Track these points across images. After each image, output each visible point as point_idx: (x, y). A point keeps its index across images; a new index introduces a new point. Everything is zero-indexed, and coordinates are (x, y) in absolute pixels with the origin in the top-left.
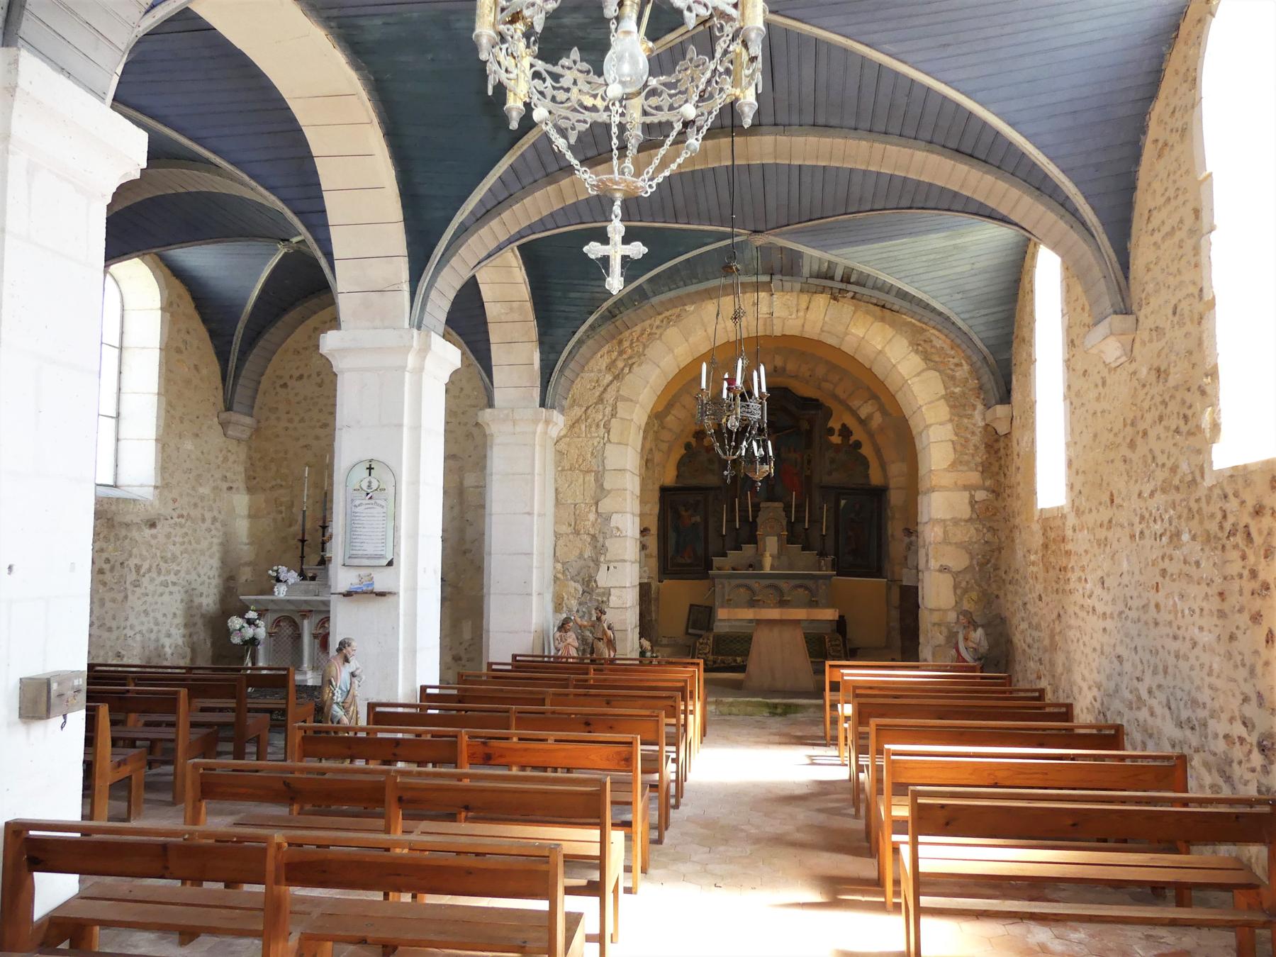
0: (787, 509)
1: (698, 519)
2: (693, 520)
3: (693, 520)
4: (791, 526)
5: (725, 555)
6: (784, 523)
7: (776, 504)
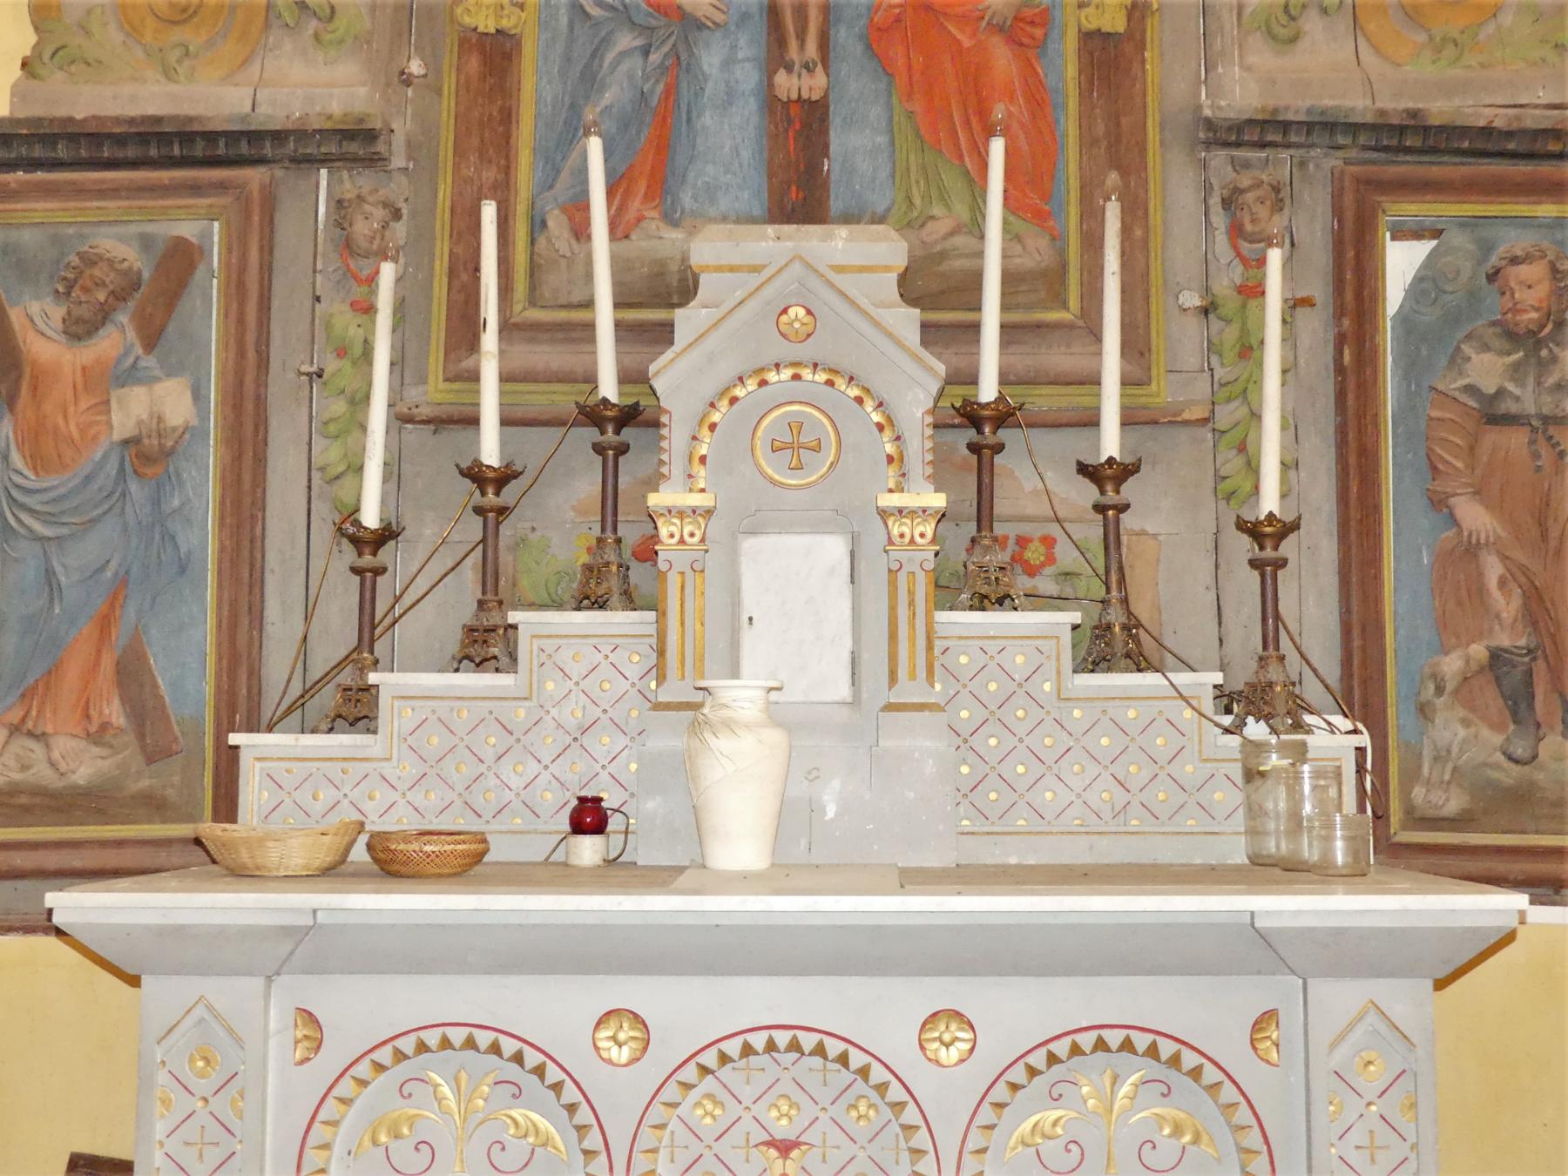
0: (938, 294)
1: (169, 401)
2: (131, 410)
3: (131, 410)
4: (976, 431)
5: (357, 710)
6: (915, 389)
7: (833, 244)
